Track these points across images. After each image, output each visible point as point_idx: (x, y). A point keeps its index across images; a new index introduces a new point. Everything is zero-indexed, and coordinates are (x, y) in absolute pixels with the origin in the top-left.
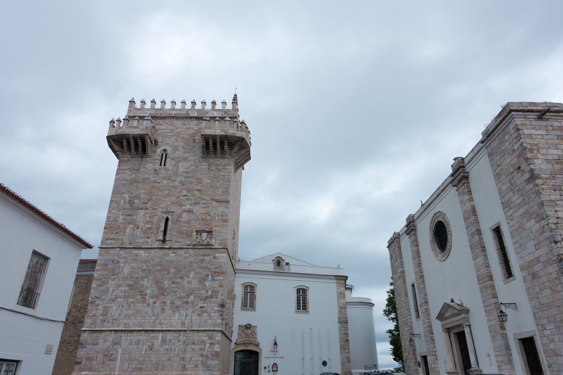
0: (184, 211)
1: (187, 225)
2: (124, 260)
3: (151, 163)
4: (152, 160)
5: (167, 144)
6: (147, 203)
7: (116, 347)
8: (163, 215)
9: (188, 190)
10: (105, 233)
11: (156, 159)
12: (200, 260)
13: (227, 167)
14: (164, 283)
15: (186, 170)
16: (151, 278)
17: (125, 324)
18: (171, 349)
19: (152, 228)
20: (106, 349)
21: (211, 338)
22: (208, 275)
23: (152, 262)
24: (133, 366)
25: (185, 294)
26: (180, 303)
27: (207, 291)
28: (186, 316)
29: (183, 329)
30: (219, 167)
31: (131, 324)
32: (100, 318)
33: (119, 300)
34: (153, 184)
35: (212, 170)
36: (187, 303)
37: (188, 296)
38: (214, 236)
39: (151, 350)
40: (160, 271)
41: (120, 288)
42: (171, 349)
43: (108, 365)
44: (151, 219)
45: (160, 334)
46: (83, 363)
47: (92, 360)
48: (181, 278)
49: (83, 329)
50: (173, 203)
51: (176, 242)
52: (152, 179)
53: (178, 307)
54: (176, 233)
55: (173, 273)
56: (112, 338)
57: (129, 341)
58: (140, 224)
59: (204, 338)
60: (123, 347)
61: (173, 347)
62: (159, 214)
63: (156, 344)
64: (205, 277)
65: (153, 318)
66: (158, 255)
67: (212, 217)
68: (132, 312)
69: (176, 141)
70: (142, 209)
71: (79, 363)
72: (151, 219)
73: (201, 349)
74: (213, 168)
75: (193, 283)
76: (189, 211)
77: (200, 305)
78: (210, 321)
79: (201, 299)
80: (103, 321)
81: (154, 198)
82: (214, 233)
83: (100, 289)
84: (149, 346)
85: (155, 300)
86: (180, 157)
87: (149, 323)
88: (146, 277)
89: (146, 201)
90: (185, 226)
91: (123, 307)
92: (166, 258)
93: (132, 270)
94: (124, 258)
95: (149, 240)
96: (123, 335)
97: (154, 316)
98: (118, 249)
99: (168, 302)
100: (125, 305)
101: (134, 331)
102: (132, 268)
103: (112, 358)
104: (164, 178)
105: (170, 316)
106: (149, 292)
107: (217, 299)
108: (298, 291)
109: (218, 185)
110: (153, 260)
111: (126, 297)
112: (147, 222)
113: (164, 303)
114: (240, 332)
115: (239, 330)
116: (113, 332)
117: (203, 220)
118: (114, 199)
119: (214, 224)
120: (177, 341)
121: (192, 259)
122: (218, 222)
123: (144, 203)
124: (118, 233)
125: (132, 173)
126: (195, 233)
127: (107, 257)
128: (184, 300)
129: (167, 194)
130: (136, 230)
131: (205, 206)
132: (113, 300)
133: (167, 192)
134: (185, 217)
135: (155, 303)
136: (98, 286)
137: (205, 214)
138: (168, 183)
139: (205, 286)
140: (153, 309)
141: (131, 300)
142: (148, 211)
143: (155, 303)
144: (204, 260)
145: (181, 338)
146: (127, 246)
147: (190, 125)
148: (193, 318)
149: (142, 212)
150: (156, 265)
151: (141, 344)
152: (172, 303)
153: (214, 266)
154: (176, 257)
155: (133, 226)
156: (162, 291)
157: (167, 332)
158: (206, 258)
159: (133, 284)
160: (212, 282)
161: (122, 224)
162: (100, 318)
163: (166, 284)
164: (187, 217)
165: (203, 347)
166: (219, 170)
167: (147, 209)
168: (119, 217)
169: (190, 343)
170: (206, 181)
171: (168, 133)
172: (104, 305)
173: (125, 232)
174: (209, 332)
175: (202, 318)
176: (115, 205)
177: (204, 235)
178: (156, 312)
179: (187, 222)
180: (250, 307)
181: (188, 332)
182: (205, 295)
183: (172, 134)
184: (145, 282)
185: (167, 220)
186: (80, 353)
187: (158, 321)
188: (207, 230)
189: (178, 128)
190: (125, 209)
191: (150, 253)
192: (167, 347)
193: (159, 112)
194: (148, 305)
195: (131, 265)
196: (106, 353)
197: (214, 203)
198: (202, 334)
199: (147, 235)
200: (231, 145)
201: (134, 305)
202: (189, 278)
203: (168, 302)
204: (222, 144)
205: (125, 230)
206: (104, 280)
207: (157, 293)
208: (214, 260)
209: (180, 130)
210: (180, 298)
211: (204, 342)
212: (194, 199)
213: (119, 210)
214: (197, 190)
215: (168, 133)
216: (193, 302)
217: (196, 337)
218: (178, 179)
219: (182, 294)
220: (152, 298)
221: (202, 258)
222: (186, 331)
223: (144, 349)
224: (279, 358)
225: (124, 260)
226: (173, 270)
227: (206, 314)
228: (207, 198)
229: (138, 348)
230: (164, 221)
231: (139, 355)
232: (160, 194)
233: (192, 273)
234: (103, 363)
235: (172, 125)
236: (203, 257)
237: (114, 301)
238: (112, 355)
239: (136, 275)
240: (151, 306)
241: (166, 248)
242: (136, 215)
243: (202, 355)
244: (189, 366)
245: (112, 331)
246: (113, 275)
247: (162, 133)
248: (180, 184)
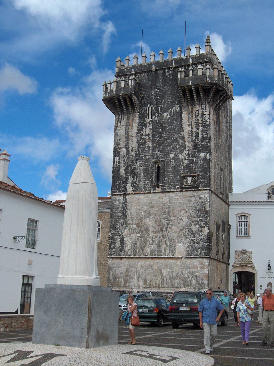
12: (188, 201)
21: (201, 263)
59: (196, 264)
75: (184, 220)
106: (151, 228)
114: (237, 257)
115: (236, 254)
121: (181, 200)
145: (178, 263)
154: (168, 199)
177: (190, 180)
180: (245, 235)
181: (183, 259)
191: (148, 197)
219: (176, 230)
236: (190, 198)
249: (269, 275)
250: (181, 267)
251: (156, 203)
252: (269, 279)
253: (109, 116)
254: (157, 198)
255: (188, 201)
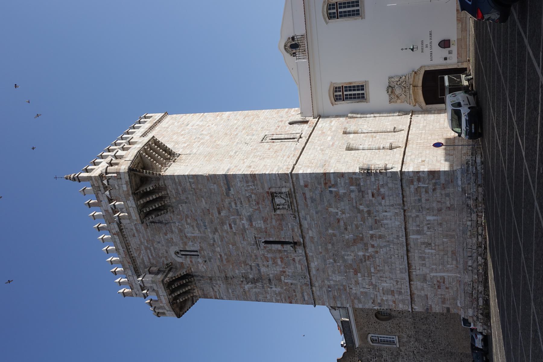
0: (251, 225)
1: (269, 221)
2: (326, 282)
3: (198, 266)
4: (193, 265)
5: (167, 252)
6: (251, 266)
7: (428, 278)
8: (262, 248)
9: (223, 223)
10: (296, 302)
11: (191, 262)
12: (312, 202)
13: (177, 180)
14: (348, 239)
15: (196, 229)
16: (343, 253)
17: (401, 272)
18: (429, 224)
19: (281, 258)
20: (432, 287)
22: (331, 192)
23: (324, 254)
24: (450, 260)
25: (359, 215)
26: (370, 220)
27: (352, 191)
28: (386, 212)
29: (403, 214)
30: (180, 190)
31: (401, 267)
32: (397, 296)
33: (374, 281)
34: (225, 262)
35: (187, 198)
36: (369, 212)
37: (360, 211)
38: (278, 190)
39: (430, 244)
40: (333, 245)
41: (360, 282)
42: (429, 224)
43: (450, 283)
44: (270, 260)
45: (411, 237)
46: (447, 306)
47: (445, 298)
48: (339, 221)
49: (410, 310)
50: (244, 238)
51: (293, 230)
52: (218, 264)
53: (376, 222)
54: (282, 232)
55: (333, 230)
56: (419, 283)
57: (421, 267)
58: (278, 270)
60: (428, 272)
61: (425, 222)
62: (261, 252)
63: (422, 240)
64: (334, 195)
65: (391, 246)
66: (313, 248)
67: (252, 193)
68: (386, 268)
69: (159, 242)
70: (259, 270)
71: (448, 309)
72: (270, 260)
73: (427, 192)
74: (183, 197)
75: (343, 208)
76: (250, 219)
77: (371, 197)
78: (390, 185)
79: (363, 197)
80: (400, 293)
81: (242, 259)
82: (273, 190)
83: (363, 300)
84: (425, 247)
85: (369, 246)
86: (180, 236)
87: (398, 250)
88: (343, 257)
89: (248, 267)
90: (271, 222)
91: (381, 277)
92: (316, 240)
93: (337, 272)
94: (323, 281)
95: (297, 259)
96: (414, 273)
97: (390, 245)
98: (314, 288)
99: (371, 232)
100: (378, 275)
101: (408, 263)
102: (334, 272)
103: (442, 281)
104: (214, 251)
105: (388, 228)
106: (361, 253)
107: (360, 179)
108: (331, 16)
109: (205, 190)
110: (321, 253)
111: (370, 275)
112: (275, 263)
113: (372, 236)
116: (412, 283)
117: (258, 203)
118: (253, 298)
119: (261, 191)
120: (418, 219)
121: (313, 212)
122: (257, 185)
123: (251, 269)
124: (294, 290)
125: (217, 284)
126: (278, 212)
127: (325, 297)
128: (366, 215)
129: (233, 245)
130: (287, 273)
131: (238, 203)
132: (375, 287)
133: (231, 246)
134: (259, 224)
135: (373, 246)
136: (360, 302)
137: (249, 201)
138: (218, 246)
139: (345, 194)
140: (381, 247)
141: (372, 270)
142: (260, 263)
143: (373, 246)
144: (311, 198)
145: (413, 215)
146: (309, 280)
147: (132, 229)
148: (387, 204)
149: (263, 270)
150: (327, 250)
151: (424, 255)
152: (371, 228)
153: (317, 185)
154: (313, 229)
155: (283, 278)
156: (358, 240)
157: (408, 231)
158: (308, 196)
159: (353, 269)
160: (339, 185)
161: (282, 288)
162: (397, 296)
163: (348, 236)
164: (259, 222)
165: (424, 190)
166: (184, 190)
167: (258, 265)
168: (275, 292)
169: (419, 204)
170: (204, 204)
171: (151, 251)
172: (382, 295)
173: (292, 284)
174: (404, 185)
175: (387, 193)
176: (261, 297)
178: (385, 244)
179: (265, 220)
181: (406, 208)
182: (357, 194)
183: (152, 248)
184: (350, 258)
185: (266, 242)
186: (437, 309)
187: (395, 241)
188: (270, 198)
189: (141, 242)
190: (263, 287)
192: (425, 228)
193: (127, 265)
194: (377, 252)
195: (330, 274)
196: (436, 287)
197: (232, 192)
198: (407, 193)
199: (291, 261)
200: (144, 180)
201: (379, 266)
202: (337, 213)
203: (371, 232)
204: (147, 194)
205: (290, 284)
206: (352, 298)
207: (360, 245)
208: (310, 186)
209: (142, 239)
210: (363, 220)
211: (417, 190)
212: (232, 215)
213: (266, 293)
214: (219, 213)
215: (151, 251)
216: (368, 206)
217: (411, 199)
218: (211, 236)
220: (367, 249)
221: (309, 201)
222: (405, 211)
223: (430, 251)
224: (431, 39)
225: (326, 282)
226: (330, 231)
227: (382, 190)
228: (227, 201)
229: (429, 258)
230: (269, 245)
231: (437, 256)
232: (235, 254)
233: (331, 209)
234: (447, 288)
235: (138, 249)
236: (307, 200)
237: (376, 286)
238: (438, 281)
239: (342, 268)
240: (378, 250)
241: (303, 241)
242: (268, 275)
243: (434, 190)
244: (448, 203)
245: (410, 284)
246: (345, 290)
247: (154, 258)
248: (217, 233)
249: (427, 47)
250: (420, 211)
251: (320, 247)
252: (433, 46)
253: (202, 308)
254: (313, 245)
255: (312, 202)
